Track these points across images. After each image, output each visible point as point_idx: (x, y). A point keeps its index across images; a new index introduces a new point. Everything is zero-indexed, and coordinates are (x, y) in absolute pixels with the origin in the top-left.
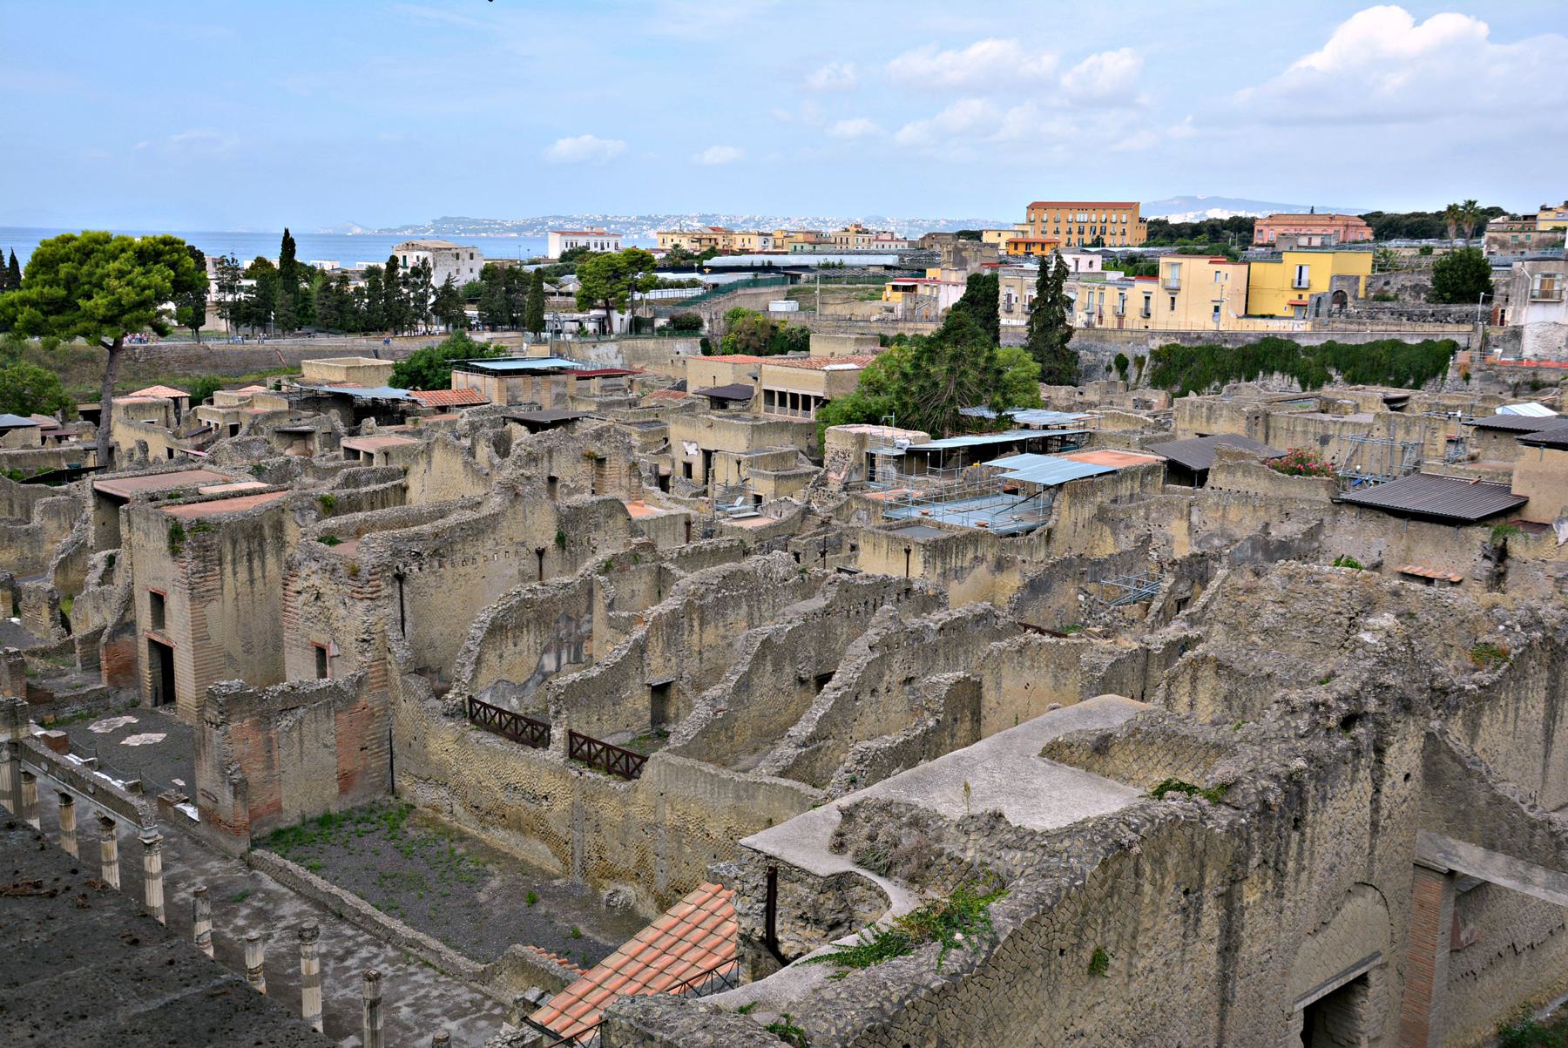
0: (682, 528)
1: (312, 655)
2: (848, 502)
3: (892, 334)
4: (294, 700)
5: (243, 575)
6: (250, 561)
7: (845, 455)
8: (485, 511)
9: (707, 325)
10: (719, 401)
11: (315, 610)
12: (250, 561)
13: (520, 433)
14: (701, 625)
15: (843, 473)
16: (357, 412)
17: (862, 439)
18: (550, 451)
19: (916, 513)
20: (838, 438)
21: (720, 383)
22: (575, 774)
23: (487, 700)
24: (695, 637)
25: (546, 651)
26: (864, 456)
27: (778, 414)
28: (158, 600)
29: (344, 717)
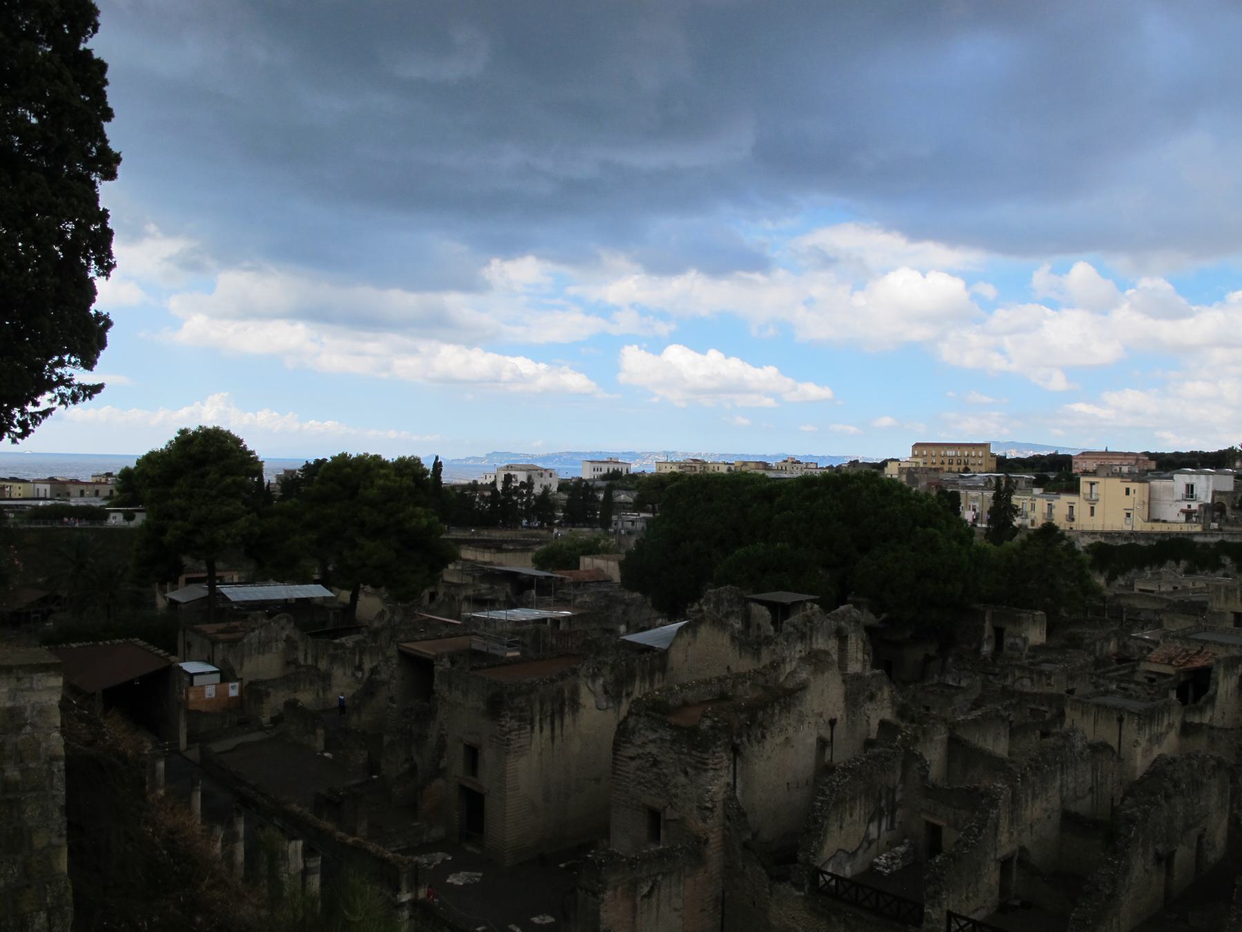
25: (871, 821)
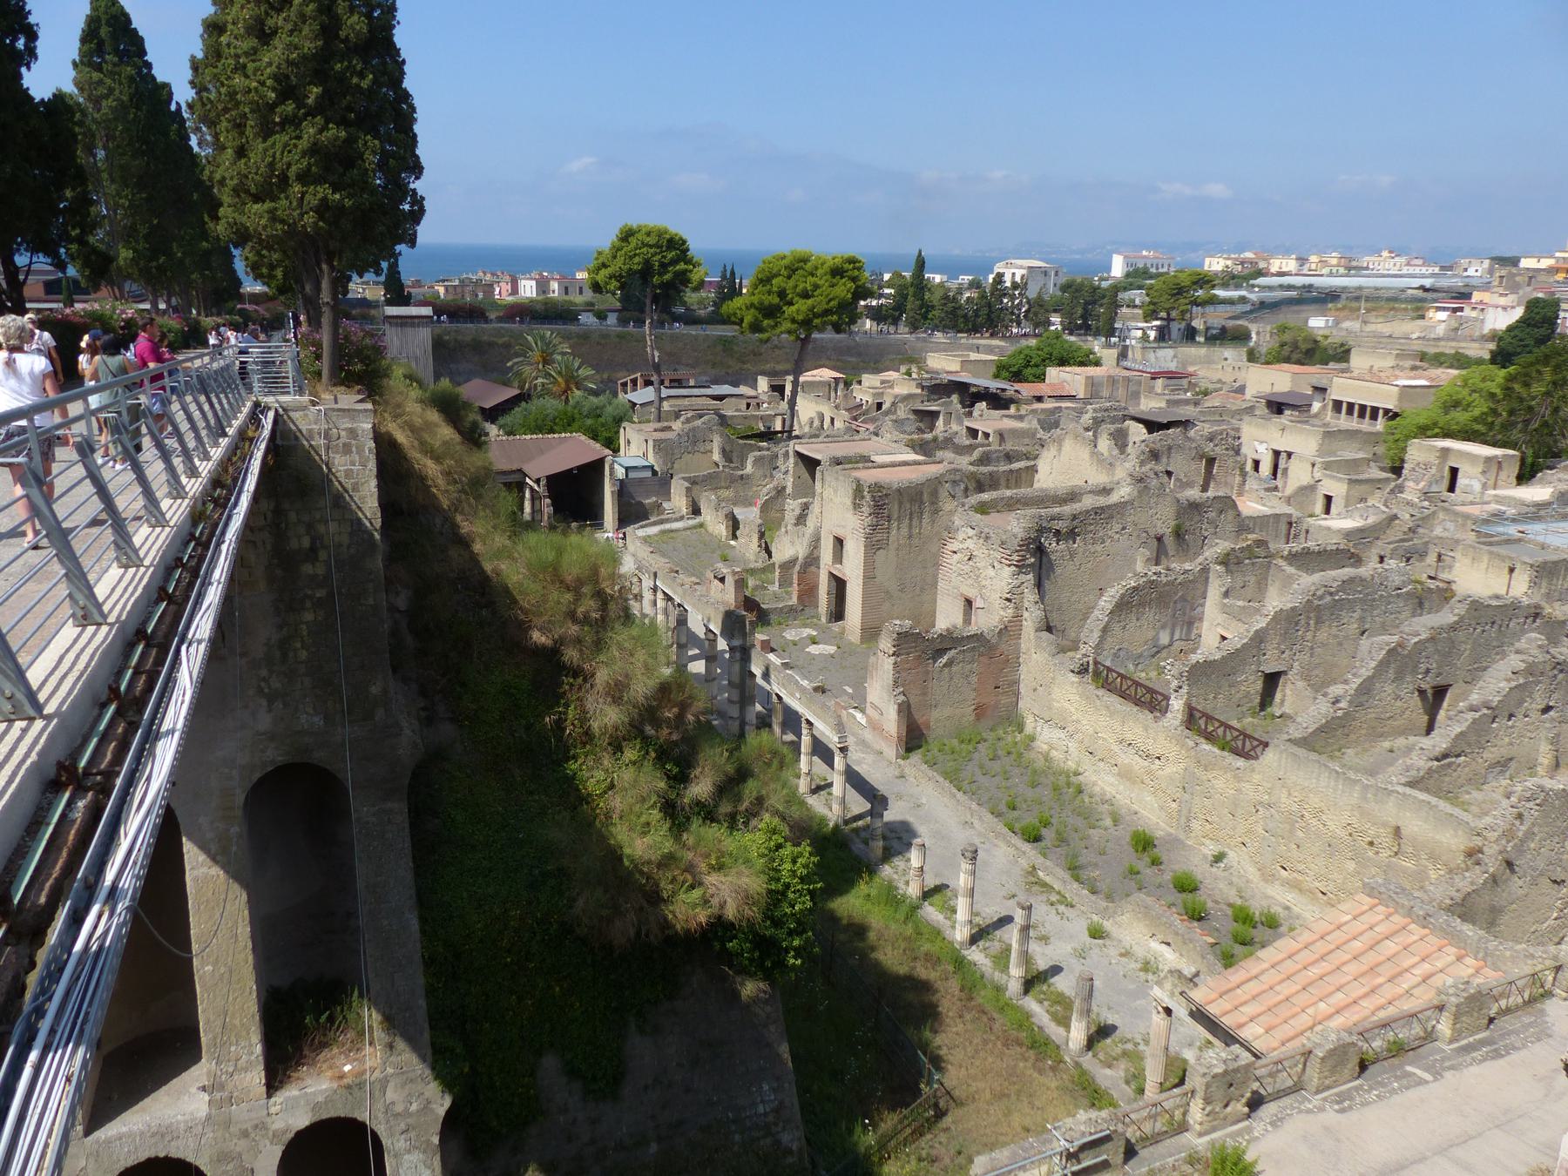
0: (1283, 527)
1: (961, 604)
2: (1434, 513)
3: (1432, 350)
4: (949, 641)
5: (905, 531)
6: (911, 519)
7: (1427, 466)
8: (1114, 498)
9: (1254, 336)
10: (1277, 407)
11: (967, 568)
12: (911, 519)
13: (1137, 432)
14: (1316, 623)
15: (1422, 484)
16: (971, 396)
17: (1445, 452)
18: (1170, 448)
19: (1512, 530)
20: (1419, 452)
21: (1277, 389)
22: (1191, 744)
23: (1108, 663)
24: (1309, 635)
25: (1163, 627)
26: (1447, 468)
27: (1353, 423)
28: (839, 542)
29: (984, 659)
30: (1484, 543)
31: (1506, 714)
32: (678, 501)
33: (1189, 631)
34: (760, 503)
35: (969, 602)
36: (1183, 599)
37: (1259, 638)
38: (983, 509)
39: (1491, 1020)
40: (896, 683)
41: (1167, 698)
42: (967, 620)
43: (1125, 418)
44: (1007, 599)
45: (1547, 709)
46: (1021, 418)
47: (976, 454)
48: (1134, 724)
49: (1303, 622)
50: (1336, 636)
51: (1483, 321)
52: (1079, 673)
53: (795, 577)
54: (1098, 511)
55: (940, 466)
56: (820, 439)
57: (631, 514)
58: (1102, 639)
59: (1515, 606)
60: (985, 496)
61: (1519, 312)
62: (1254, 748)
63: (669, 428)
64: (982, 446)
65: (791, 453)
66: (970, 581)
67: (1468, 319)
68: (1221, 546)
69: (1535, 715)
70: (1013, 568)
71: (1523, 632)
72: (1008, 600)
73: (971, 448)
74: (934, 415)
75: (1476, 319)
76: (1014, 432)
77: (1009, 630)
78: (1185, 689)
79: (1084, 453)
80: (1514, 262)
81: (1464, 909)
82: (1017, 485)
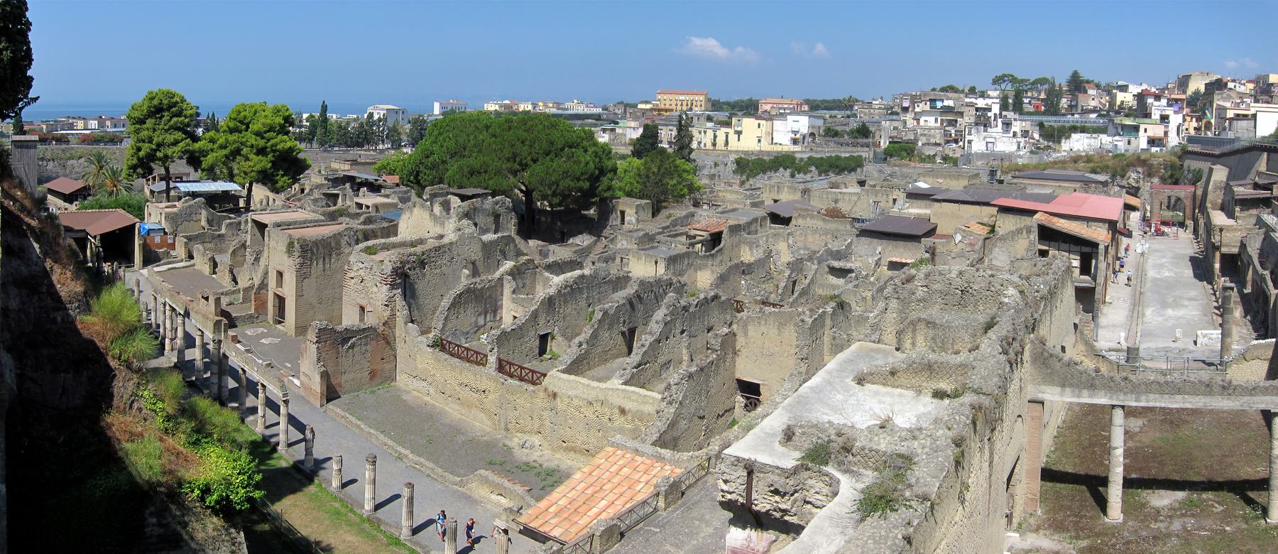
13: (455, 201)
28: (280, 274)
30: (642, 250)
31: (665, 338)
32: (180, 251)
33: (495, 316)
34: (231, 251)
35: (362, 309)
36: (490, 297)
37: (535, 315)
38: (370, 251)
39: (683, 494)
40: (319, 360)
41: (486, 356)
42: (362, 320)
43: (448, 194)
44: (386, 305)
45: (683, 332)
46: (387, 196)
47: (362, 219)
48: (468, 373)
49: (557, 303)
50: (575, 309)
51: (625, 135)
52: (432, 346)
53: (253, 296)
54: (437, 249)
55: (340, 226)
56: (268, 211)
57: (150, 258)
58: (444, 325)
59: (658, 282)
60: (370, 243)
61: (641, 131)
62: (538, 378)
63: (175, 206)
64: (366, 213)
65: (249, 220)
66: (362, 296)
67: (619, 134)
68: (509, 265)
69: (678, 336)
70: (388, 286)
71: (666, 294)
72: (386, 305)
73: (358, 215)
74: (336, 196)
75: (622, 134)
76: (384, 205)
77: (389, 323)
78: (496, 350)
79: (426, 215)
80: (635, 106)
81: (661, 442)
82: (388, 236)
